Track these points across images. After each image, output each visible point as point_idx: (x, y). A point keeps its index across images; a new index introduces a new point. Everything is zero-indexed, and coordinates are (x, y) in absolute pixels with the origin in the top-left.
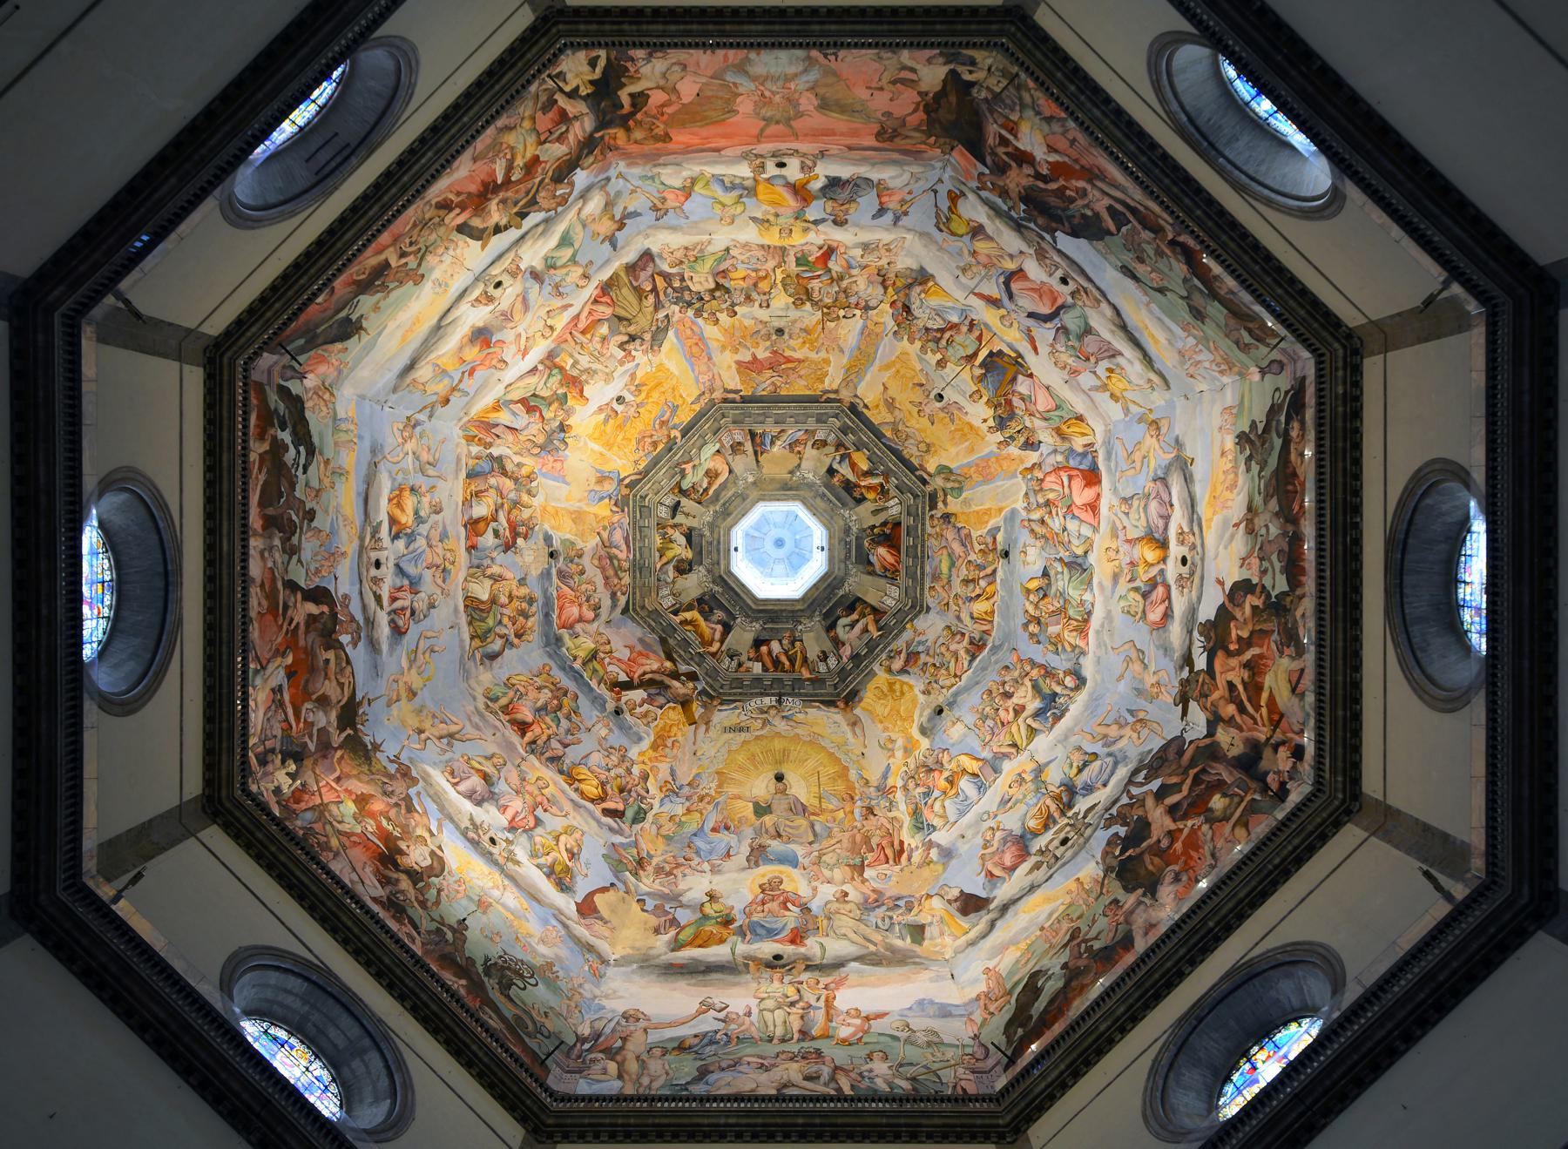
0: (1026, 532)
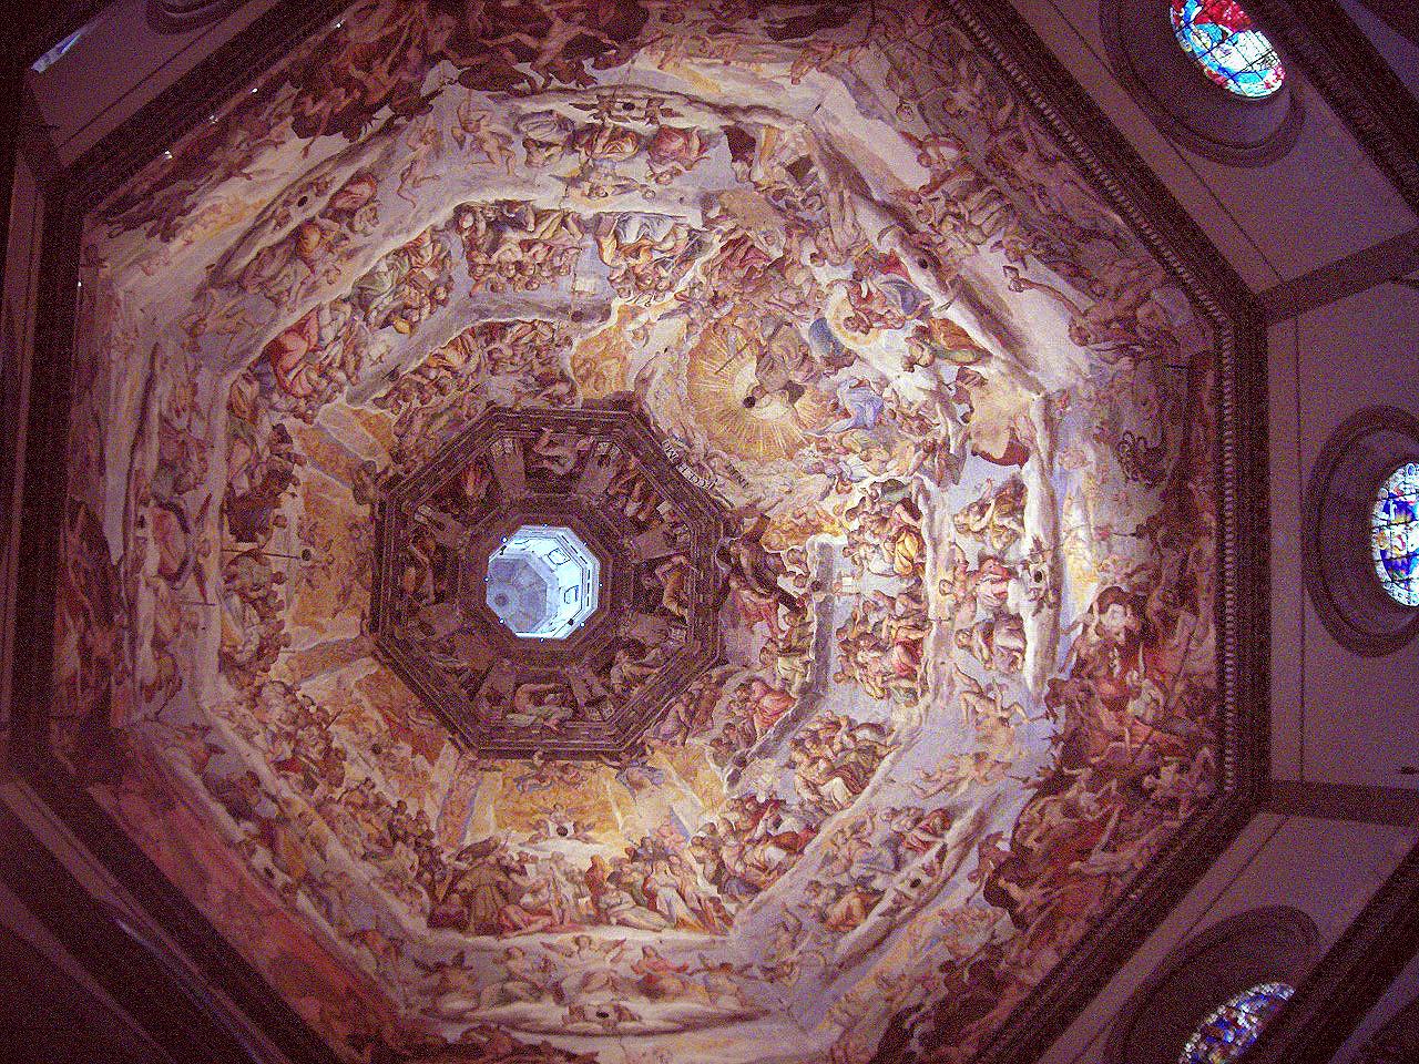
0: (362, 373)
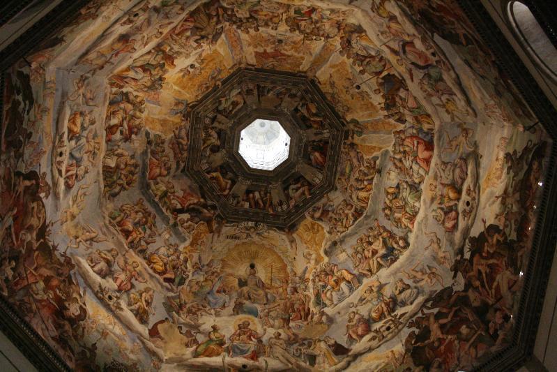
0: (392, 163)
